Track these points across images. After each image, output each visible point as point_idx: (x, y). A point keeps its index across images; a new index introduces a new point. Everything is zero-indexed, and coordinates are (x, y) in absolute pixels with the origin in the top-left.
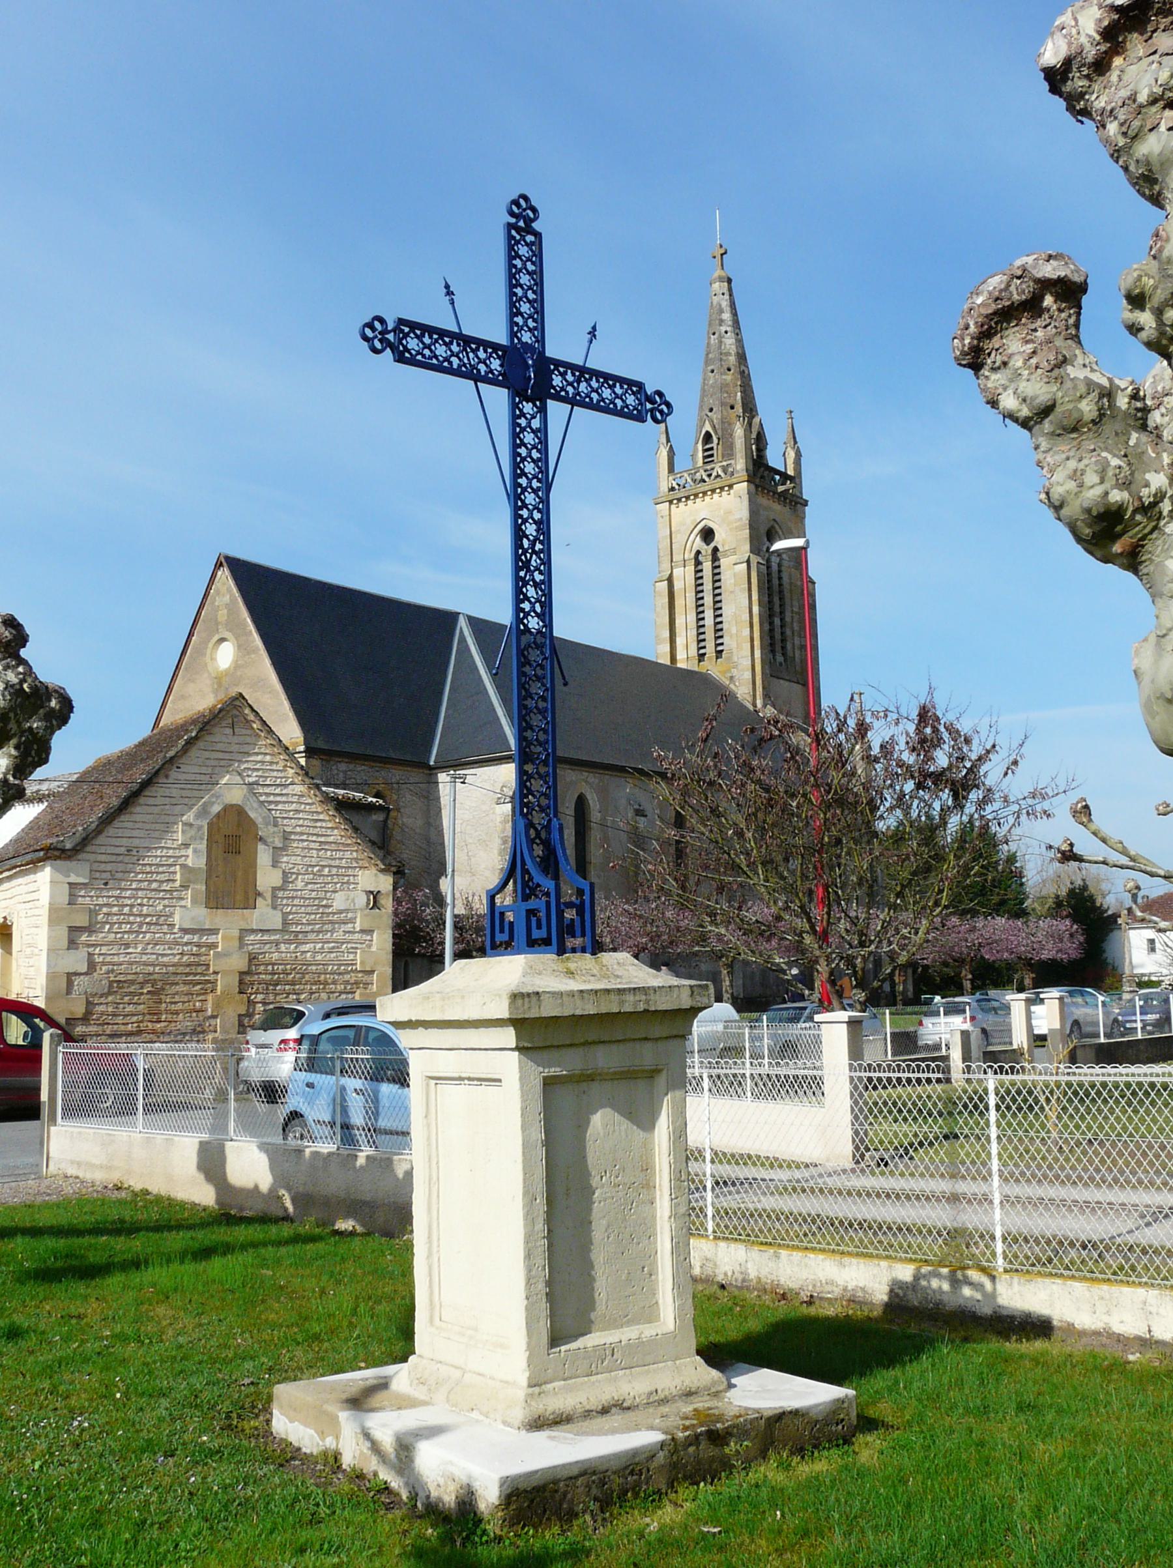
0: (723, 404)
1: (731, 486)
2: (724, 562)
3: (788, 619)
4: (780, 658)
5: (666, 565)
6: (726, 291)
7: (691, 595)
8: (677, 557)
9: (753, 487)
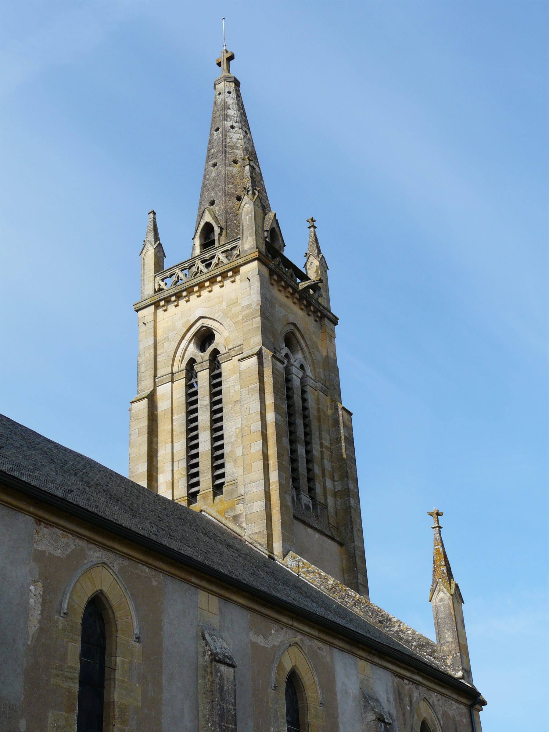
0: (227, 194)
1: (236, 270)
2: (226, 368)
3: (316, 453)
4: (306, 500)
7: (180, 418)
9: (265, 270)
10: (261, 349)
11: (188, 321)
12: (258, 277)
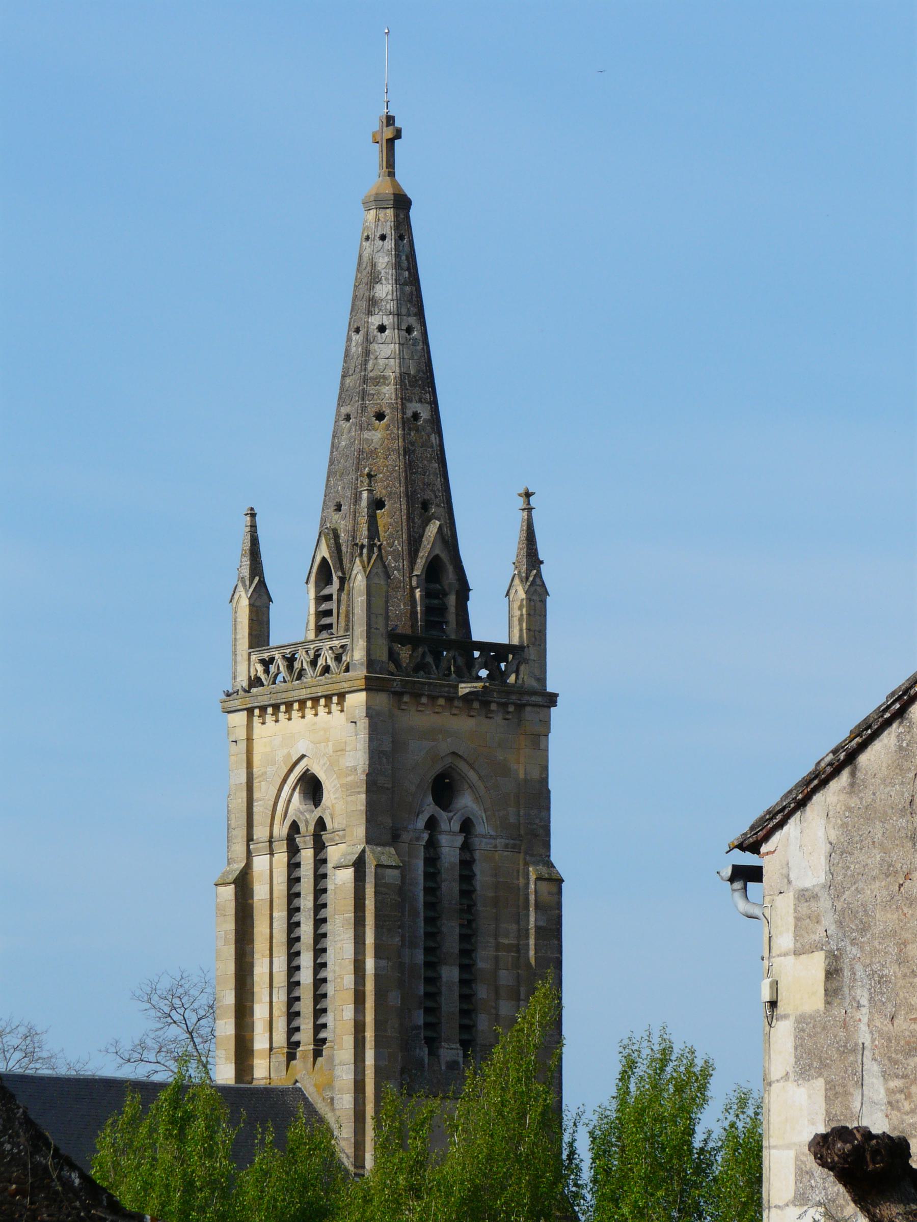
5: (240, 849)
6: (388, 228)
7: (281, 915)
8: (261, 833)
10: (363, 851)
11: (289, 755)
12: (367, 720)
